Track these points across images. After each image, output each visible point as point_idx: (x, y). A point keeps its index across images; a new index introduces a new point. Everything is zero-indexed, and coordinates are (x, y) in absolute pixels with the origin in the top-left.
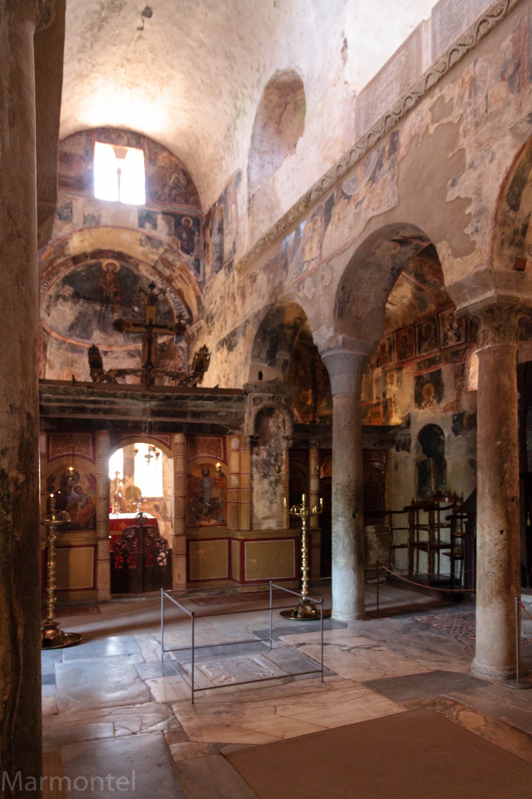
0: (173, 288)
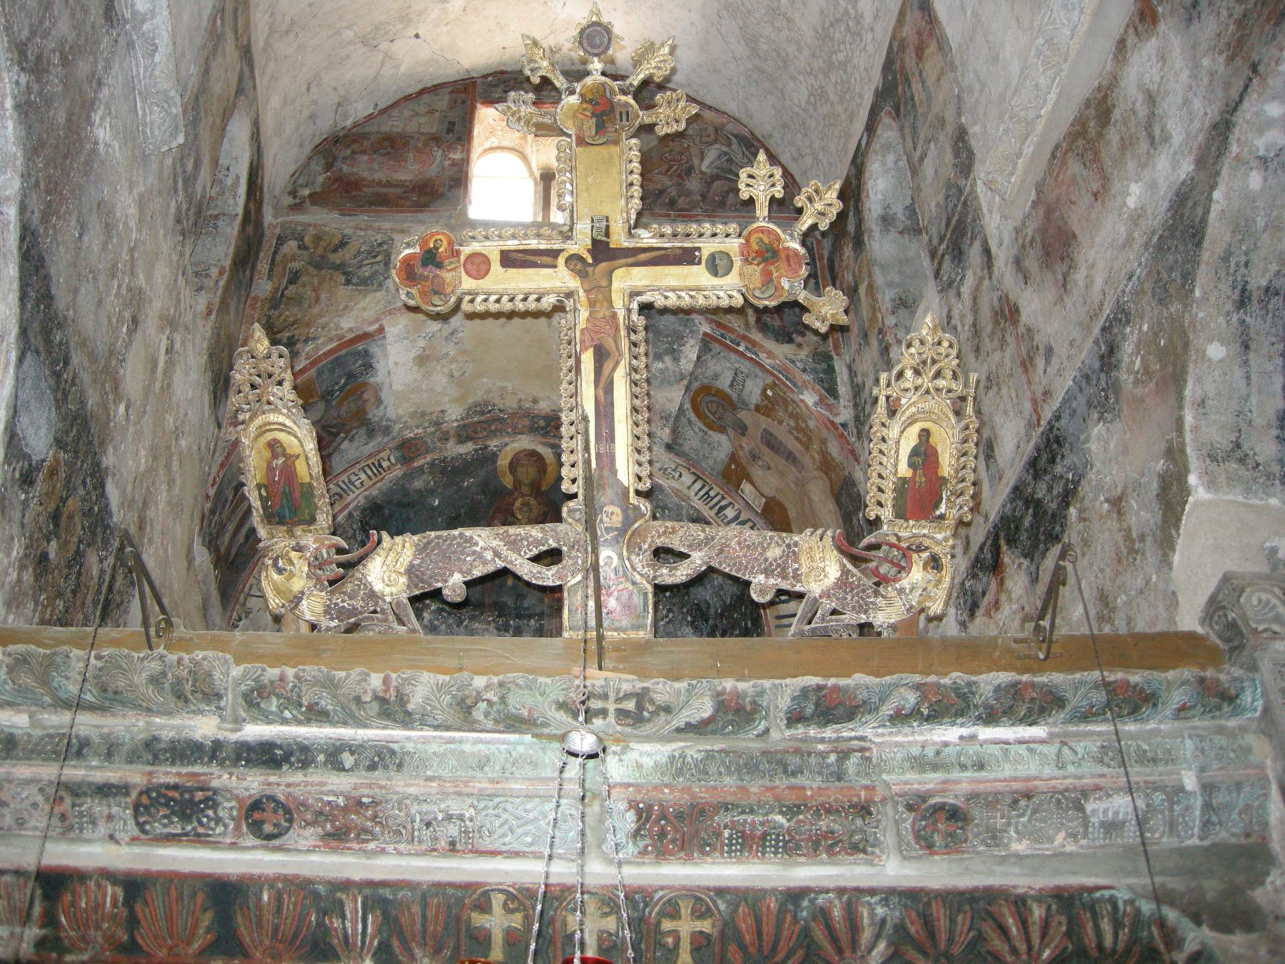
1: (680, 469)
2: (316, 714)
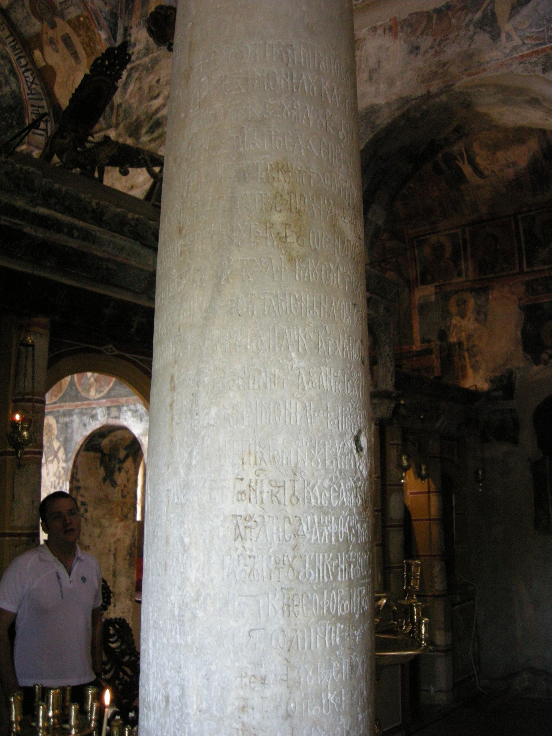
0: (33, 61)
1: (4, 25)
2: (68, 210)
